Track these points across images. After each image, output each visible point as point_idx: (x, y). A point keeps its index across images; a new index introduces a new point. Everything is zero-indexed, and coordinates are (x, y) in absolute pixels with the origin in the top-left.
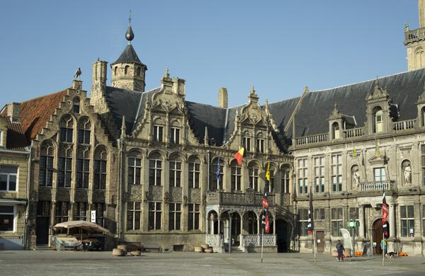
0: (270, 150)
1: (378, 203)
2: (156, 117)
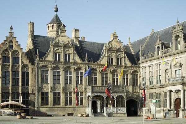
0: (125, 63)
1: (176, 89)
2: (56, 49)
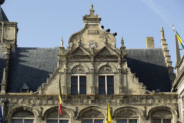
0: (124, 89)
